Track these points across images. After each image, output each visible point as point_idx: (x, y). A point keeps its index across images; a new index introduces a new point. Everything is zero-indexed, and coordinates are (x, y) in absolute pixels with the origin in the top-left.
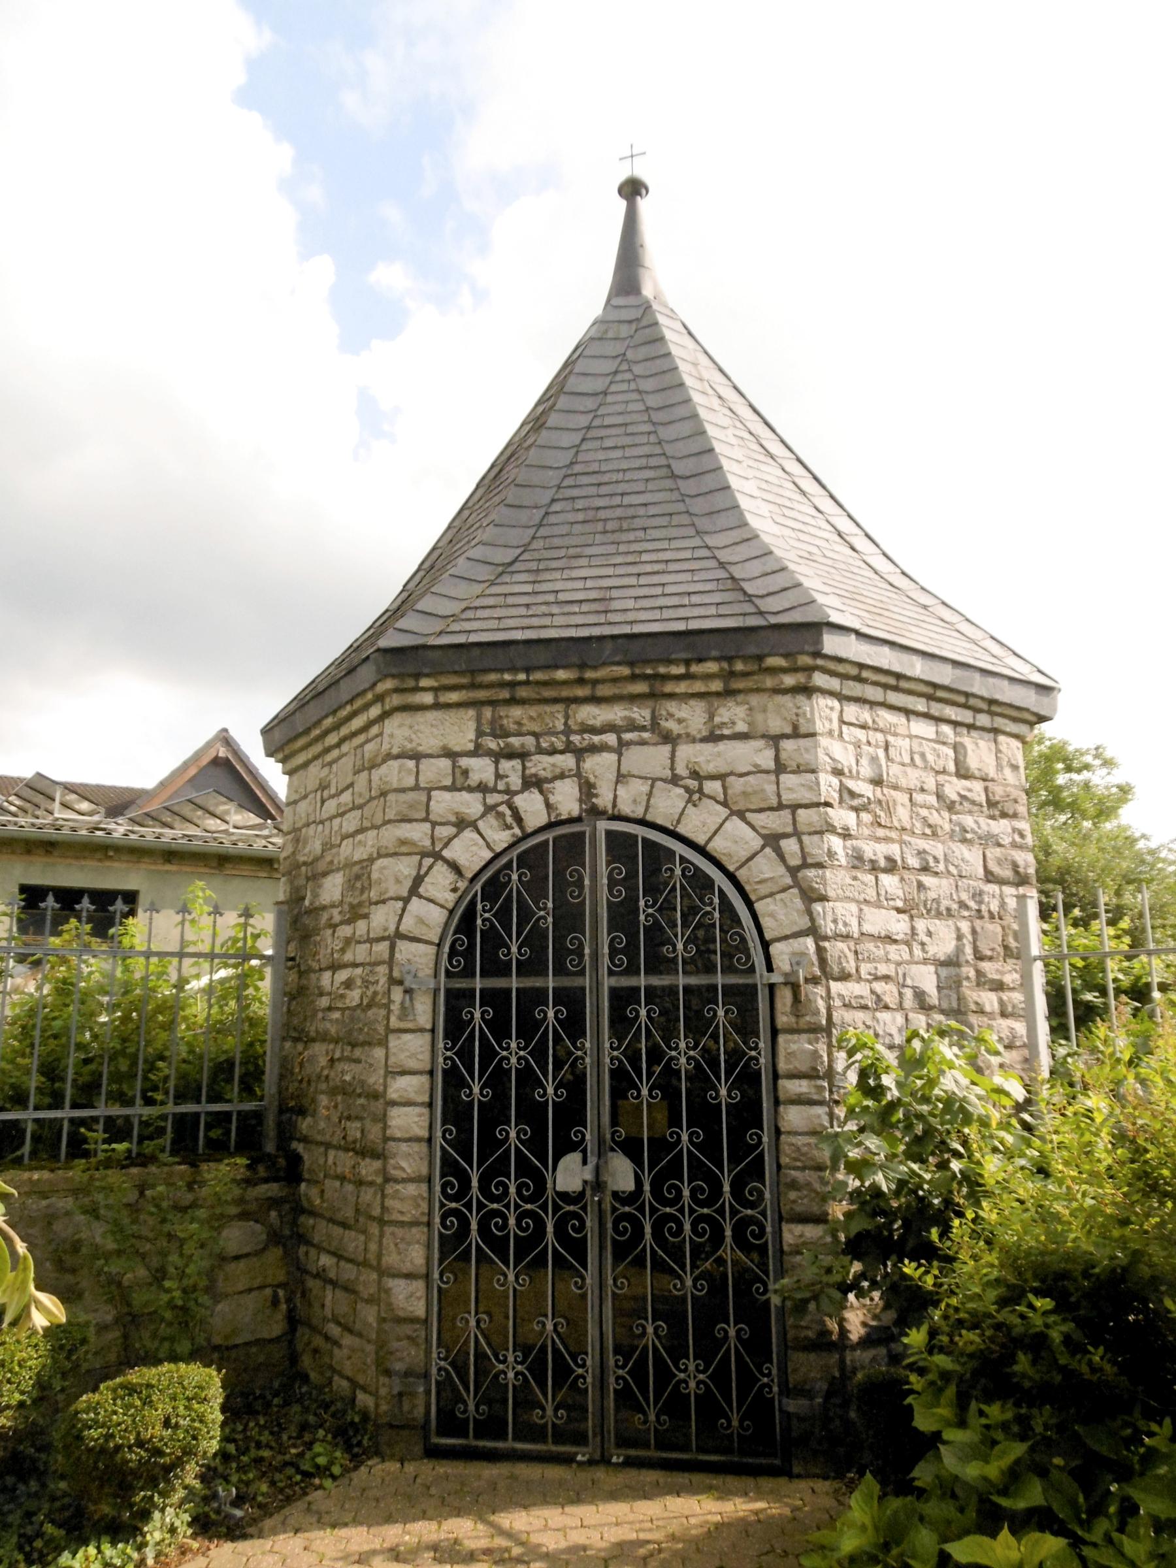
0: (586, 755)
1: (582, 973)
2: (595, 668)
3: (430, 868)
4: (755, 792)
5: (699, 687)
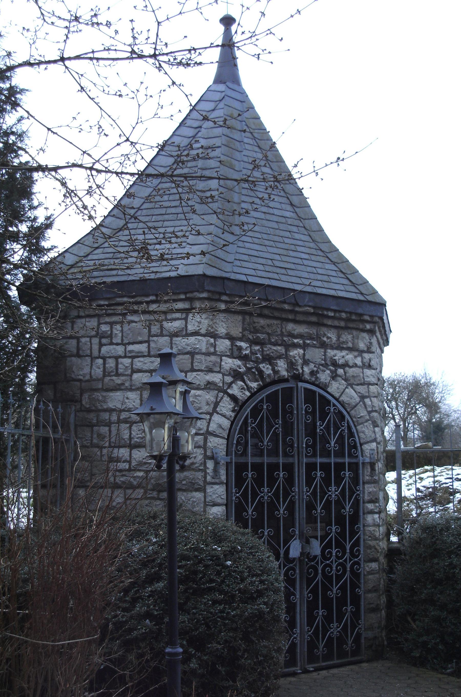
0: (290, 348)
1: (293, 456)
2: (300, 306)
3: (222, 398)
4: (357, 376)
5: (336, 323)
